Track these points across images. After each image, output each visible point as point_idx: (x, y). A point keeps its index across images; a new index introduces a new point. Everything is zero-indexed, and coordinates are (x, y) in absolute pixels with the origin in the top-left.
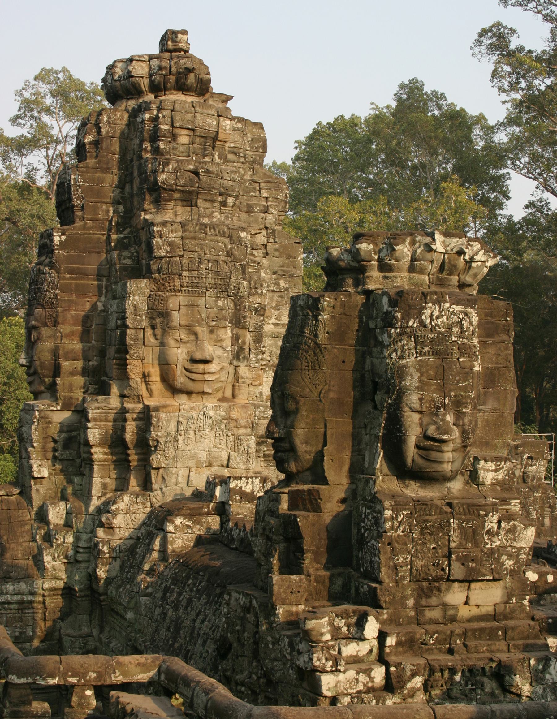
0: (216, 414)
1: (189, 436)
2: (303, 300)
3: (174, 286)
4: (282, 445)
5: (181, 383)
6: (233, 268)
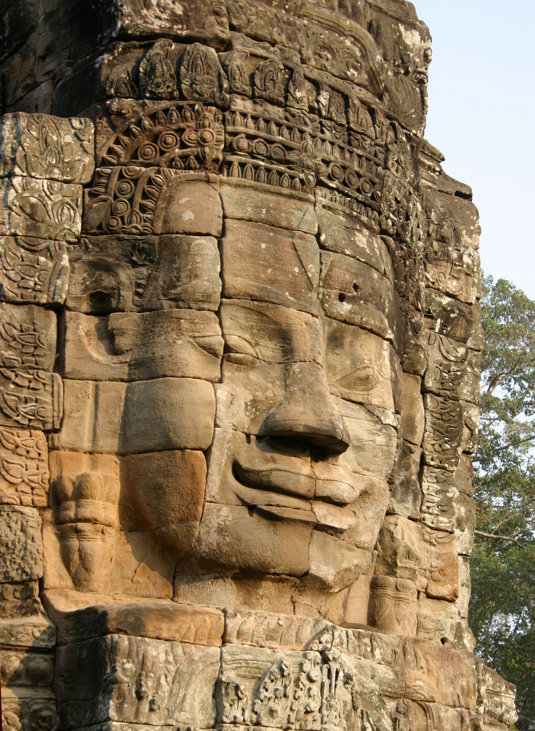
3: (202, 142)
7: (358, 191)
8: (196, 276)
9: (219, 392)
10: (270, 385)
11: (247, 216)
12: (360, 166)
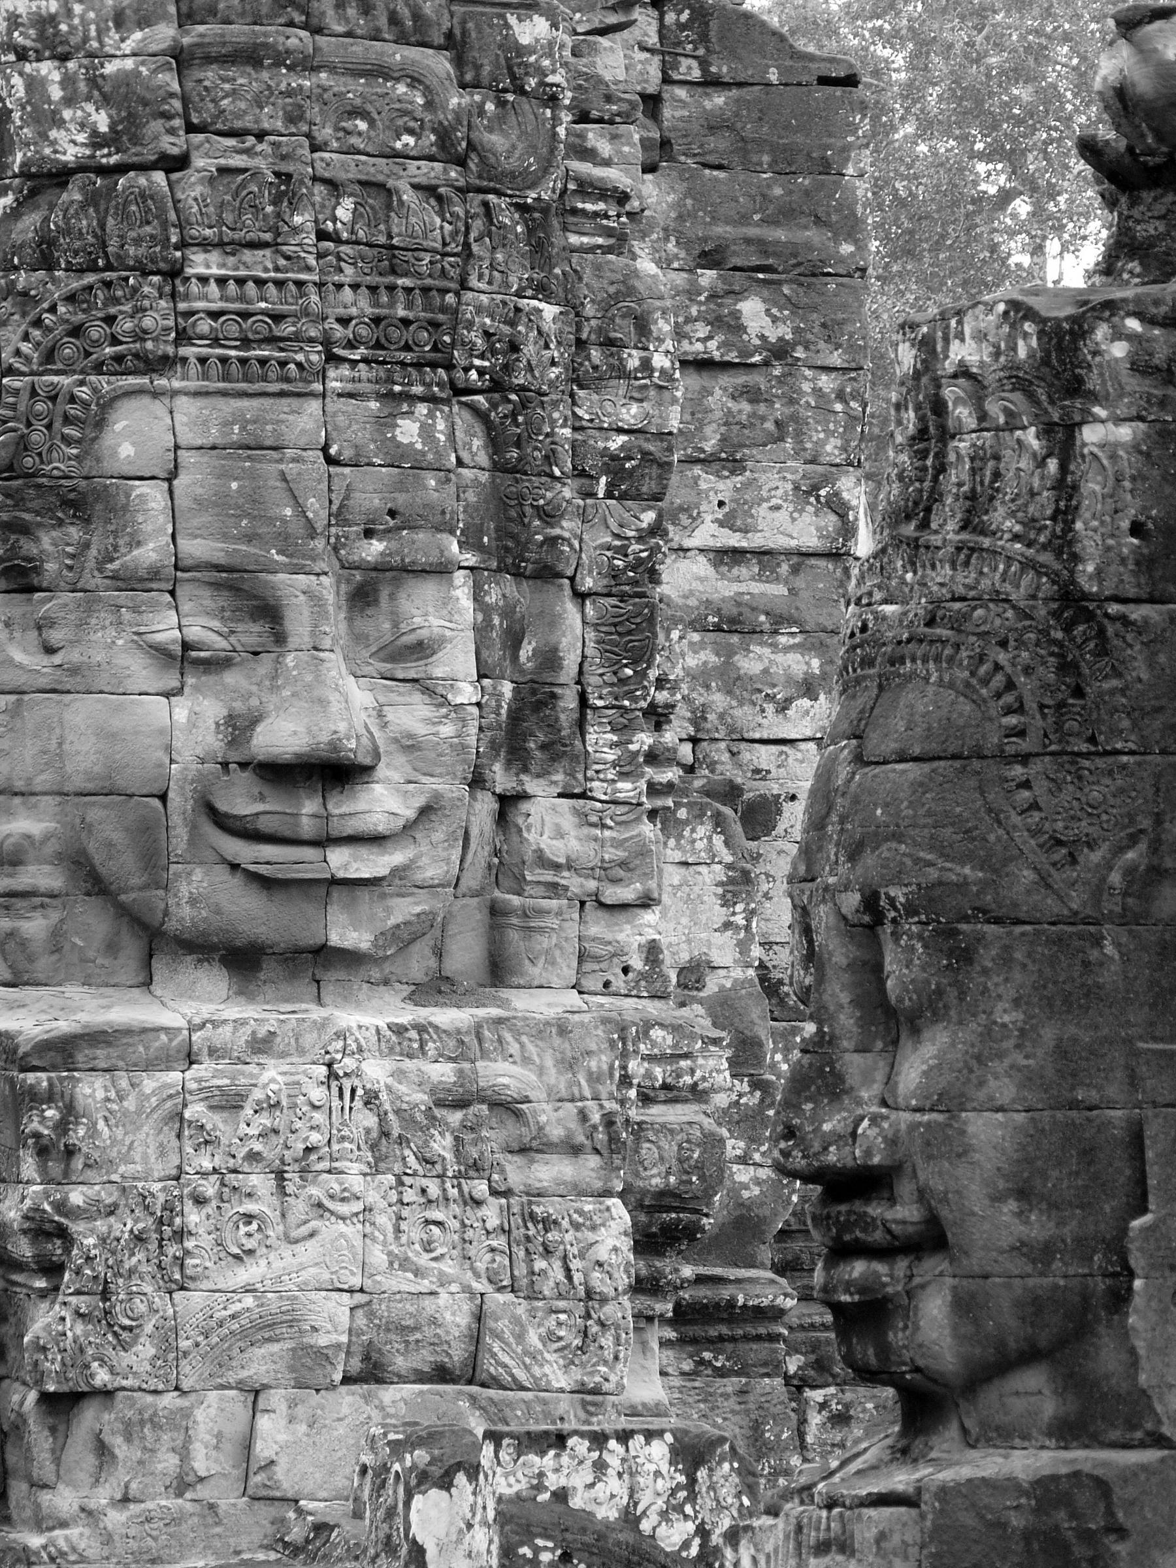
0: (399, 1074)
1: (250, 1207)
2: (981, 336)
4: (875, 1210)
5: (193, 901)
6: (478, 225)
7: (407, 348)
8: (139, 544)
9: (177, 710)
10: (254, 688)
11: (210, 441)
12: (409, 306)
